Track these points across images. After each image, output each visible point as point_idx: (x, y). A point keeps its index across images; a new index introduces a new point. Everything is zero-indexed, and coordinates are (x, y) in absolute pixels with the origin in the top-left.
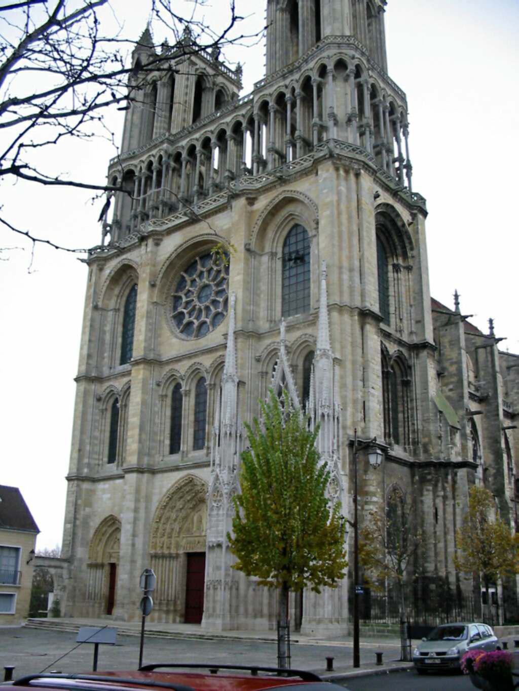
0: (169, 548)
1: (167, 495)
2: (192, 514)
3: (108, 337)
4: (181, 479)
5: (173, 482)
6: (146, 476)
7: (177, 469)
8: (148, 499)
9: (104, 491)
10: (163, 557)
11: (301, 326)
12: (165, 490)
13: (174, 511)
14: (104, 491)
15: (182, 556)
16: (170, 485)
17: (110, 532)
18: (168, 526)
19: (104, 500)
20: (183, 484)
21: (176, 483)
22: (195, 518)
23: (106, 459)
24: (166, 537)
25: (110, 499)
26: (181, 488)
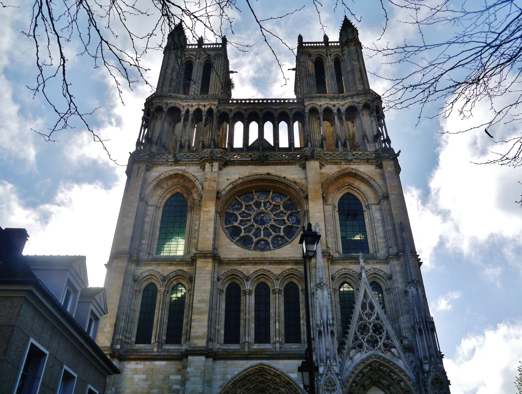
3: (147, 228)
4: (251, 367)
5: (241, 369)
6: (211, 360)
11: (371, 262)
12: (229, 377)
14: (136, 371)
16: (236, 373)
19: (136, 380)
20: (252, 372)
21: (245, 371)
23: (134, 339)
25: (146, 380)
26: (246, 377)
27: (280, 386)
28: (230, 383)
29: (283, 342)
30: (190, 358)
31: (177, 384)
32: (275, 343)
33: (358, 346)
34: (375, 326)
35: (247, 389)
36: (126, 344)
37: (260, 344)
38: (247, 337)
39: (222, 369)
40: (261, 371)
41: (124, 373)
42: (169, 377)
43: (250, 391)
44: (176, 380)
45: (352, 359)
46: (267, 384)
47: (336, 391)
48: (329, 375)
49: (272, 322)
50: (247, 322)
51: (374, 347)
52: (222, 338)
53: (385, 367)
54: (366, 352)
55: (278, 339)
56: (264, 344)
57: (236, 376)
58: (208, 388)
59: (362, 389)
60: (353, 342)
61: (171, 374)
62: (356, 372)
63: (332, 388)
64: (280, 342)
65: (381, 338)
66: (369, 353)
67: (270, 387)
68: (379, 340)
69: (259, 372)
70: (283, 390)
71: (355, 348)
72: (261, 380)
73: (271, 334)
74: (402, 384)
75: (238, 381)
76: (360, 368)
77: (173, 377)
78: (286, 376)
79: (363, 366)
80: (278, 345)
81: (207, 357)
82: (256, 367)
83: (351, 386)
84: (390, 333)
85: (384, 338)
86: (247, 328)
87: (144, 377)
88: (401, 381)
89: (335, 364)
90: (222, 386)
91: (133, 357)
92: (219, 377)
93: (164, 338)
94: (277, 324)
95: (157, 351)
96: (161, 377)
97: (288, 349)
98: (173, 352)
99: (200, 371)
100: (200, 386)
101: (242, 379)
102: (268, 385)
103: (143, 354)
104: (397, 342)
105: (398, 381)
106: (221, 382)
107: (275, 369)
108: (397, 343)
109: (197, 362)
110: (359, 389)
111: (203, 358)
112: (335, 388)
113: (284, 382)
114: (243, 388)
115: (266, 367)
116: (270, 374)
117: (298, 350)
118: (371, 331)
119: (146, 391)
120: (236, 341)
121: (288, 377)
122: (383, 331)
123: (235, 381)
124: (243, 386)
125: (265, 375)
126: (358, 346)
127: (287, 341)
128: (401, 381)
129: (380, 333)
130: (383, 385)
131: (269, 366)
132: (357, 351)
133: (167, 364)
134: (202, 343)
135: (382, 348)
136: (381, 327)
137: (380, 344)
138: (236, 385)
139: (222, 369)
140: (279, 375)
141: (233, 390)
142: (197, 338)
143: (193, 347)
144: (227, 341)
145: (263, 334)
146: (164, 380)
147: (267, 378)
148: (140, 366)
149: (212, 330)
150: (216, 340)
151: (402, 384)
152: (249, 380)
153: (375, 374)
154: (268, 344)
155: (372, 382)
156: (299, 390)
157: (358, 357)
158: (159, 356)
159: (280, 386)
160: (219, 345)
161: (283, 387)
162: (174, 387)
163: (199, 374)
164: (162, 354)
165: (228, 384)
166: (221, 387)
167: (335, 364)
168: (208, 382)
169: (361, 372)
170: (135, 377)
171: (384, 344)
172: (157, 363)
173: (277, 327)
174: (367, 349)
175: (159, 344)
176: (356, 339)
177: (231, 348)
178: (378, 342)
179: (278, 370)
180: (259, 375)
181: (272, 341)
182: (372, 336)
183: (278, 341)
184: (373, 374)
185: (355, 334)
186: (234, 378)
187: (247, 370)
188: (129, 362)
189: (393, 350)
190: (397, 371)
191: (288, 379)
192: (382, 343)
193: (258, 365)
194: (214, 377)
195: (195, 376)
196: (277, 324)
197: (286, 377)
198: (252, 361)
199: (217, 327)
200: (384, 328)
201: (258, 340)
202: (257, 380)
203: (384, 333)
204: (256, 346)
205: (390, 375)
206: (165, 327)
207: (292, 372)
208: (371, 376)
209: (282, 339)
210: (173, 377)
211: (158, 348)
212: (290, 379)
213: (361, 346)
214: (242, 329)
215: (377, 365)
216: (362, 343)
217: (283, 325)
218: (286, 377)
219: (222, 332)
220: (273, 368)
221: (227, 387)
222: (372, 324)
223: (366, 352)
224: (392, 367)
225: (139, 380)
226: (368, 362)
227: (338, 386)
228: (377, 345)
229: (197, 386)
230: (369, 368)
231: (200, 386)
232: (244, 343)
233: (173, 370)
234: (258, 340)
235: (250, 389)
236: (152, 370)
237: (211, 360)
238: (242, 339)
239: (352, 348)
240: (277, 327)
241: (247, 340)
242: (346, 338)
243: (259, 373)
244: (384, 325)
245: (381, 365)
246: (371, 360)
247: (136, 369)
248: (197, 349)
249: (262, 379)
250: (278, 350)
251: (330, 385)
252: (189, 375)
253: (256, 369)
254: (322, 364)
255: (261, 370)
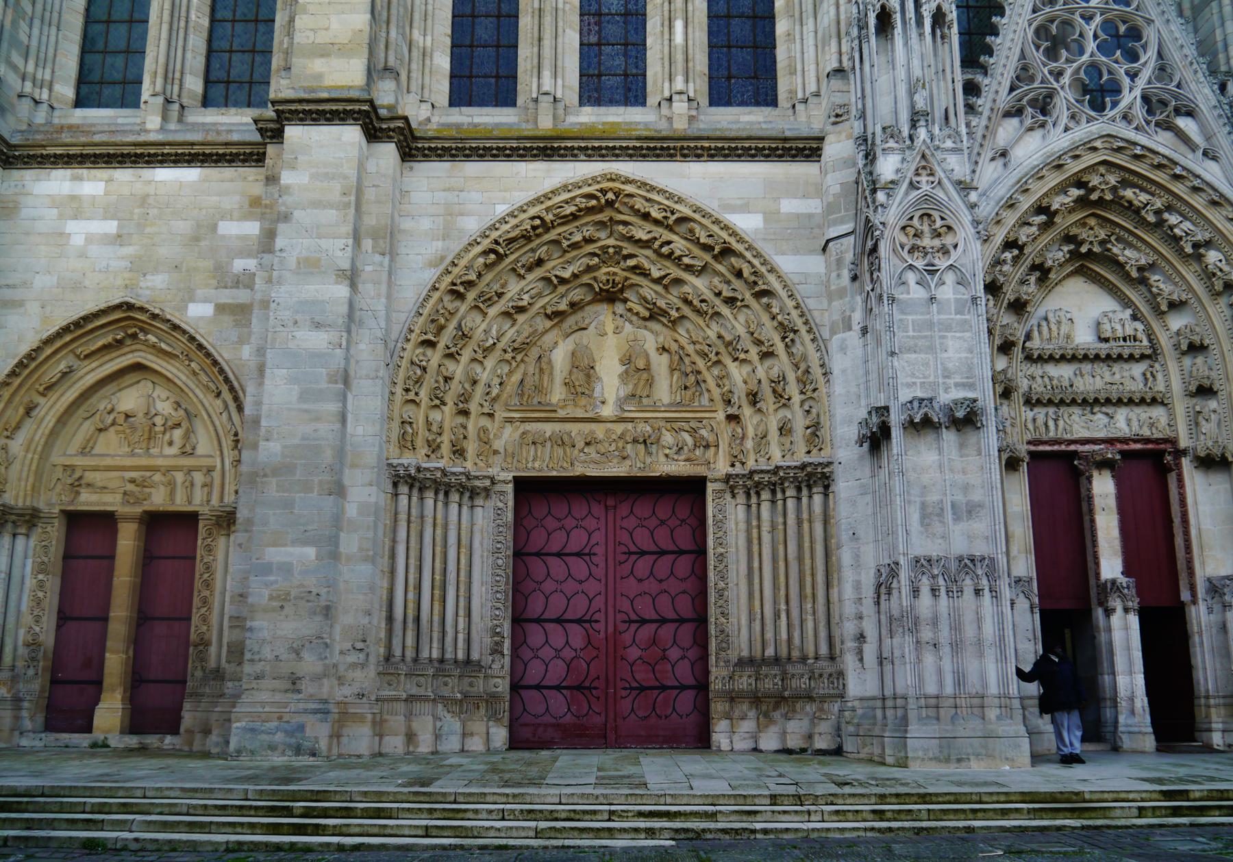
0: (459, 452)
1: (486, 244)
2: (548, 339)
4: (565, 188)
5: (521, 197)
6: (388, 152)
7: (547, 148)
8: (389, 240)
9: (75, 208)
10: (443, 486)
12: (472, 225)
13: (493, 311)
14: (75, 208)
15: (510, 488)
16: (501, 209)
17: (90, 379)
18: (457, 370)
19: (78, 241)
20: (569, 209)
21: (538, 201)
22: (560, 357)
23: (67, 91)
24: (448, 409)
25: (119, 239)
26: (547, 227)
27: (688, 268)
28: (479, 249)
29: (704, 101)
30: (293, 132)
31: (244, 253)
32: (670, 99)
33: (1033, 103)
34: (1108, 25)
35: (547, 280)
36: (26, 104)
37: (603, 109)
38: (547, 74)
39: (441, 196)
40: (603, 205)
41: (25, 212)
42: (214, 228)
43: (562, 289)
44: (244, 238)
45: (1004, 154)
46: (631, 262)
47: (954, 255)
48: (925, 187)
49: (653, 25)
50: (548, 20)
51: (1099, 107)
52: (441, 88)
53: (1142, 189)
54: (1066, 129)
55: (679, 84)
56: (621, 109)
57: (503, 221)
58: (378, 258)
59: (1033, 279)
60: (1012, 89)
61: (223, 218)
62: (1026, 203)
63: (937, 243)
64: (689, 100)
65: (1133, 76)
66: (1083, 131)
67: (645, 274)
68: (1126, 81)
69: (600, 209)
70: (699, 285)
71: (1018, 112)
72: (604, 249)
73: (649, 74)
74: (1212, 256)
75: (511, 241)
76: (1039, 190)
77: (230, 228)
78: (717, 222)
79: (1054, 179)
80: (680, 106)
81: (373, 134)
82: (586, 190)
83: (998, 262)
84: (1175, 56)
85: (1146, 74)
86: (547, 42)
87: (111, 227)
88: (1208, 244)
89: (949, 144)
90: (442, 259)
91: (59, 151)
92: (426, 224)
93: (195, 84)
94: (679, 25)
95: (162, 129)
96: (183, 227)
97: (724, 125)
98: (231, 131)
99: (337, 187)
100: (340, 243)
101: (527, 238)
102: (637, 270)
103: (97, 138)
104: (1207, 91)
105: (1196, 246)
106: (440, 244)
107: (670, 196)
108: (1203, 93)
109: (322, 154)
110: (1023, 282)
111: (352, 134)
112: (948, 240)
113: (707, 248)
114: (530, 277)
115: (629, 189)
116: (646, 216)
117: (764, 126)
118: (1091, 46)
119: (119, 282)
120: (505, 95)
121: (726, 228)
122: (1144, 47)
123: (497, 242)
124: (530, 269)
125: (625, 223)
126: (1033, 103)
127: (720, 95)
128: (1208, 244)
129: (1133, 57)
130: (1121, 266)
131: (643, 185)
132: (1028, 122)
133: (205, 180)
134: (345, 75)
135: (1139, 111)
136: (1135, 33)
137: (1130, 97)
138: (500, 257)
139: (441, 196)
140: (684, 220)
141: (488, 277)
142: (323, 51)
143: (305, 89)
144: (459, 98)
145: (613, 66)
146: (196, 239)
147: (630, 239)
148: (93, 184)
149: (393, 33)
150: (414, 86)
151: (1212, 256)
152: (556, 242)
153: (1092, 222)
154: (639, 109)
155: (1075, 255)
156: (771, 278)
157: (1032, 149)
158: (170, 144)
159: (688, 268)
160: (427, 102)
161: (701, 271)
162: (239, 265)
163: (336, 196)
164: (180, 137)
165: (466, 250)
166: (433, 264)
167: (949, 144)
168: (377, 236)
169: (1041, 209)
170: (72, 226)
171: (1146, 99)
172: (165, 175)
173: (679, 38)
174: (1073, 117)
175: (168, 101)
176: (1024, 74)
177: (477, 120)
178: (1118, 91)
179: (680, 200)
180: (602, 224)
181: (652, 100)
182: (1094, 67)
183: (680, 93)
184: (1082, 223)
185: (1023, 56)
186: (493, 227)
187: (547, 197)
188: (43, 173)
189: (1183, 123)
190: (1198, 202)
191: (724, 235)
192: (1137, 92)
193: (595, 180)
194: (407, 224)
195: (317, 204)
196: (679, 25)
197: (715, 228)
198: (571, 165)
199: (416, 35)
200: (1150, 34)
201: (594, 90)
202: (590, 248)
203: (1149, 58)
204: (589, 116)
205: (1161, 223)
206: (197, 43)
207: (745, 208)
208: (1074, 231)
209: (699, 87)
210: (230, 228)
211: (165, 118)
212: (734, 234)
213: (1043, 105)
214: (525, 52)
215: (1112, 179)
216: (1050, 95)
217: (700, 37)
218: (715, 228)
219: (443, 62)
220: (661, 191)
221: (463, 263)
222: (1098, 19)
223: (1066, 129)
224: (1178, 188)
225: (90, 239)
226: (1074, 167)
227: (965, 233)
228: (1115, 104)
229: (324, 243)
230: (1075, 193)
231: (340, 243)
232: (536, 100)
233: (231, 202)
234: (594, 90)
235: (563, 281)
236: (144, 200)
237: (388, 152)
238: (527, 85)
239: (1008, 114)
240: (679, 38)
241: (547, 85)
242: (985, 70)
243: (599, 217)
244: (1150, 22)
245: (1130, 179)
246: (1090, 159)
247: (73, 198)
248: (325, 95)
249: (611, 242)
250: (680, 125)
251: (926, 228)
252: (287, 199)
253: (590, 196)
254: (891, 144)
255: (610, 204)
